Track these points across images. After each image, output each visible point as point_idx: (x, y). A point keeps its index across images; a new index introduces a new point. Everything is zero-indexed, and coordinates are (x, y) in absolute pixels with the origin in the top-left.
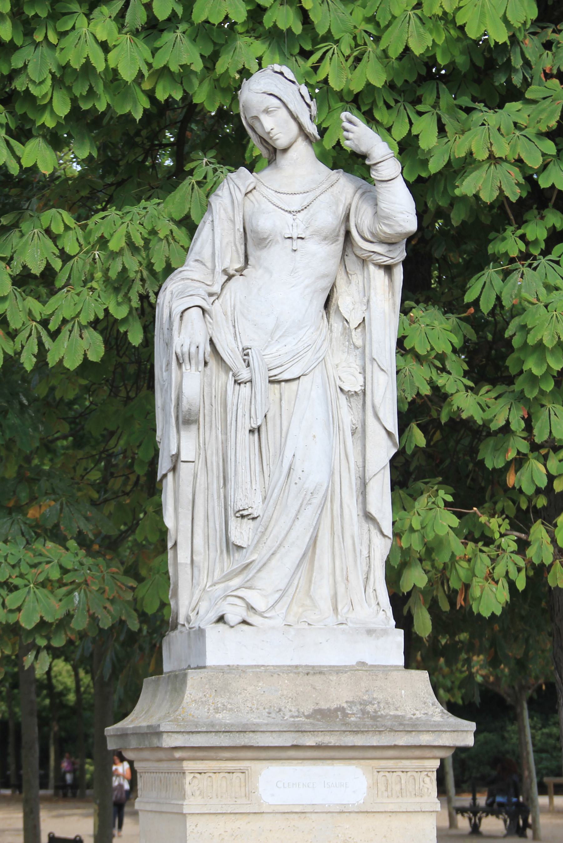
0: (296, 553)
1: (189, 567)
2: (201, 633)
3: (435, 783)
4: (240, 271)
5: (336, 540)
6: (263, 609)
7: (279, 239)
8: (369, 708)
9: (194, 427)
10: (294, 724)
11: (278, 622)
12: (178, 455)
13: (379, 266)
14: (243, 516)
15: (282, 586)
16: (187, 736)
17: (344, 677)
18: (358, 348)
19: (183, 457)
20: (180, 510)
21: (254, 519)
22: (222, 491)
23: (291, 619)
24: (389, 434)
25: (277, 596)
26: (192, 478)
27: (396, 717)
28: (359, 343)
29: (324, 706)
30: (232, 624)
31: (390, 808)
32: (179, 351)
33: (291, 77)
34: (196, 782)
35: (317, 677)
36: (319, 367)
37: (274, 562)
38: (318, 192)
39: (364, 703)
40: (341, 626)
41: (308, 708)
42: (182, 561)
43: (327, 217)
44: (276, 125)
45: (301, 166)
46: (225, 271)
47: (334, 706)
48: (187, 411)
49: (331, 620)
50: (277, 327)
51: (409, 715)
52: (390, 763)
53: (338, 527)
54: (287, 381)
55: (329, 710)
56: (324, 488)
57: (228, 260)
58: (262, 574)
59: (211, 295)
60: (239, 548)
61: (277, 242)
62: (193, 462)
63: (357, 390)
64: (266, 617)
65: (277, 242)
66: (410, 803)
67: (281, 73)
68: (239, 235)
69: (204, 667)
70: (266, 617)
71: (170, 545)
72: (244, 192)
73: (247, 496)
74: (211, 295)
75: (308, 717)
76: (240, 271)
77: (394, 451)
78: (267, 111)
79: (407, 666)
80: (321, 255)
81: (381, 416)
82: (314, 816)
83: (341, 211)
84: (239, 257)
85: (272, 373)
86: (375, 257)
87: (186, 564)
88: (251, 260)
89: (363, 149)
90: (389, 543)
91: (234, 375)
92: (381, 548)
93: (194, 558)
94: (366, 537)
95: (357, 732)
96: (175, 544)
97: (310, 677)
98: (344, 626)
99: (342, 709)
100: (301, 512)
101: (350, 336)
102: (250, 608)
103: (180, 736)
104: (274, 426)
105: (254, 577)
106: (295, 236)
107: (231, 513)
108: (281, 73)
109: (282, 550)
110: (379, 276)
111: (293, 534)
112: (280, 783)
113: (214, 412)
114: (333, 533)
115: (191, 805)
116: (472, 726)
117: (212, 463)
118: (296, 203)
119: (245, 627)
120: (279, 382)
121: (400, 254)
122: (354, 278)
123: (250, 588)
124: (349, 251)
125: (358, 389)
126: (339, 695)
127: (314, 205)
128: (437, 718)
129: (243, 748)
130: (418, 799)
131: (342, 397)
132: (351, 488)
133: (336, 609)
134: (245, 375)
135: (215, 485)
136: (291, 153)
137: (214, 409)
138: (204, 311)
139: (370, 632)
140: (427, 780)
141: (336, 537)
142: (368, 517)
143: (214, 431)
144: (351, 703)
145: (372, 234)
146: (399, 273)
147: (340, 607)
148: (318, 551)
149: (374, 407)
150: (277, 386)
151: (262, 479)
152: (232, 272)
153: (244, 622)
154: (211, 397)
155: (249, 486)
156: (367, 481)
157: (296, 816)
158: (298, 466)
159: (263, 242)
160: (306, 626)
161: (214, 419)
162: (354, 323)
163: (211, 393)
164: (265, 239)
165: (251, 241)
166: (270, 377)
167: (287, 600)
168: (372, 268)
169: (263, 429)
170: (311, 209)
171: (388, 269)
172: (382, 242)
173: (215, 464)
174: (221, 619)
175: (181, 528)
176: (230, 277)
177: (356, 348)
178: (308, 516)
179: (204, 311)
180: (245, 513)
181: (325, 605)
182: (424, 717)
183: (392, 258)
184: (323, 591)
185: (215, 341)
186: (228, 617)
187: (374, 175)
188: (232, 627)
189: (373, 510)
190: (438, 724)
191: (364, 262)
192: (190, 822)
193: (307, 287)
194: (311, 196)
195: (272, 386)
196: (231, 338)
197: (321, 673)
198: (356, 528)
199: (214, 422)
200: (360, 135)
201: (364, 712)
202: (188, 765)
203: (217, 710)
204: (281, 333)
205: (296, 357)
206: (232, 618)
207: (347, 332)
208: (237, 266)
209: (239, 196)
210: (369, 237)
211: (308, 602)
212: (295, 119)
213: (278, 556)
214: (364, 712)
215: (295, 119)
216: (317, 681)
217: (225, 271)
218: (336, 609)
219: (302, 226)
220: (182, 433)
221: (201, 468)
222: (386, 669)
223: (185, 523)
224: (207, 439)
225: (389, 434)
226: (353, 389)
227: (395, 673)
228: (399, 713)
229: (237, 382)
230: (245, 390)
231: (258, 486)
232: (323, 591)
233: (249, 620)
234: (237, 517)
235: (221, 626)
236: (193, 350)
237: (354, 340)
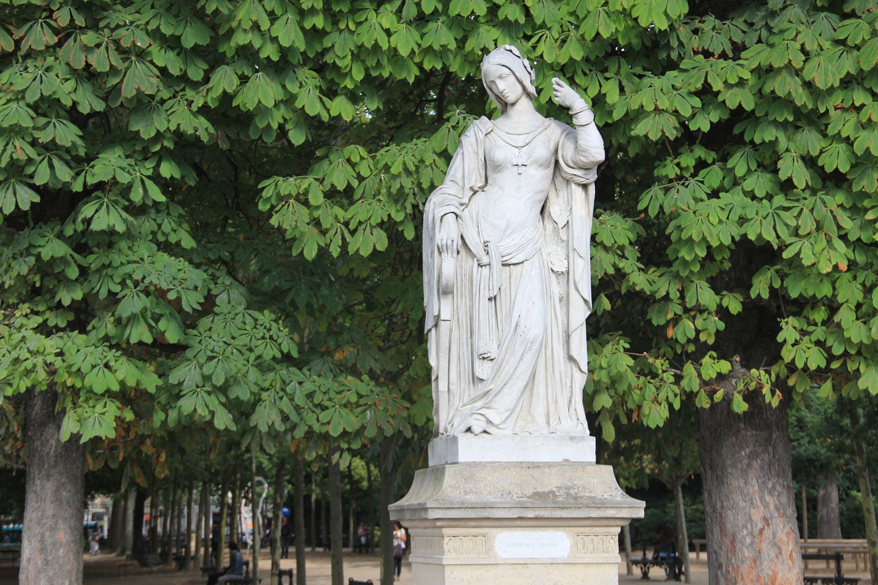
0: (521, 384)
2: (455, 439)
3: (617, 543)
4: (482, 188)
7: (509, 166)
8: (572, 492)
9: (450, 297)
10: (519, 502)
11: (508, 432)
12: (438, 316)
13: (579, 185)
14: (484, 358)
15: (511, 407)
16: (445, 511)
17: (554, 470)
19: (442, 318)
20: (440, 354)
21: (491, 360)
23: (517, 430)
24: (586, 301)
25: (508, 413)
27: (590, 497)
28: (564, 238)
29: (540, 490)
31: (586, 561)
32: (439, 244)
33: (518, 53)
34: (451, 542)
35: (536, 469)
36: (537, 256)
37: (505, 390)
38: (536, 133)
39: (568, 488)
41: (529, 491)
43: (542, 151)
44: (508, 88)
45: (524, 114)
46: (471, 188)
47: (547, 490)
49: (545, 431)
50: (507, 227)
51: (600, 497)
52: (586, 530)
53: (550, 366)
54: (514, 264)
55: (544, 493)
56: (541, 338)
57: (474, 180)
58: (497, 398)
59: (462, 205)
60: (482, 380)
61: (508, 168)
65: (508, 168)
66: (600, 557)
67: (511, 51)
68: (482, 163)
69: (457, 463)
71: (433, 378)
72: (484, 133)
73: (487, 343)
74: (462, 205)
75: (529, 498)
76: (482, 188)
77: (589, 313)
78: (500, 77)
79: (598, 462)
80: (539, 177)
81: (580, 288)
82: (533, 566)
83: (552, 146)
85: (504, 259)
86: (576, 179)
89: (567, 103)
90: (585, 377)
91: (478, 261)
92: (580, 381)
94: (569, 373)
95: (563, 508)
96: (437, 377)
97: (531, 470)
99: (553, 492)
101: (558, 233)
102: (489, 422)
103: (440, 511)
106: (520, 164)
107: (475, 356)
108: (511, 51)
109: (511, 382)
110: (578, 191)
111: (519, 371)
112: (509, 543)
114: (546, 370)
115: (447, 559)
116: (643, 504)
118: (520, 141)
119: (486, 435)
120: (509, 265)
121: (593, 176)
122: (561, 193)
123: (488, 408)
124: (557, 174)
125: (564, 270)
126: (551, 482)
127: (533, 142)
128: (619, 499)
129: (484, 519)
130: (605, 555)
131: (553, 276)
132: (559, 339)
133: (548, 423)
134: (485, 260)
136: (518, 107)
138: (457, 216)
139: (572, 439)
140: (612, 541)
142: (571, 359)
144: (559, 488)
145: (574, 162)
146: (592, 190)
148: (536, 383)
149: (575, 282)
150: (507, 268)
152: (476, 189)
153: (485, 432)
157: (521, 566)
158: (522, 324)
159: (498, 168)
160: (528, 434)
162: (561, 224)
164: (499, 166)
165: (490, 167)
167: (514, 416)
168: (573, 186)
169: (498, 298)
170: (531, 145)
171: (585, 187)
172: (580, 168)
174: (469, 430)
176: (475, 192)
177: (563, 241)
178: (529, 357)
179: (457, 216)
180: (485, 356)
181: (541, 420)
182: (610, 498)
184: (539, 410)
185: (465, 236)
186: (474, 428)
187: (575, 121)
189: (574, 354)
190: (620, 503)
191: (568, 182)
192: (447, 570)
193: (528, 199)
194: (531, 136)
195: (504, 268)
196: (476, 235)
197: (538, 467)
198: (562, 367)
200: (564, 93)
201: (568, 494)
202: (445, 531)
203: (466, 493)
205: (520, 248)
206: (477, 429)
207: (556, 230)
208: (480, 185)
209: (481, 136)
210: (571, 164)
211: (529, 418)
212: (520, 82)
213: (508, 386)
214: (568, 494)
215: (520, 82)
216: (536, 472)
217: (471, 188)
218: (548, 423)
219: (525, 157)
220: (442, 301)
222: (584, 464)
223: (444, 363)
225: (586, 301)
226: (560, 270)
227: (589, 467)
228: (592, 495)
230: (486, 270)
232: (539, 410)
233: (488, 430)
235: (469, 434)
236: (449, 243)
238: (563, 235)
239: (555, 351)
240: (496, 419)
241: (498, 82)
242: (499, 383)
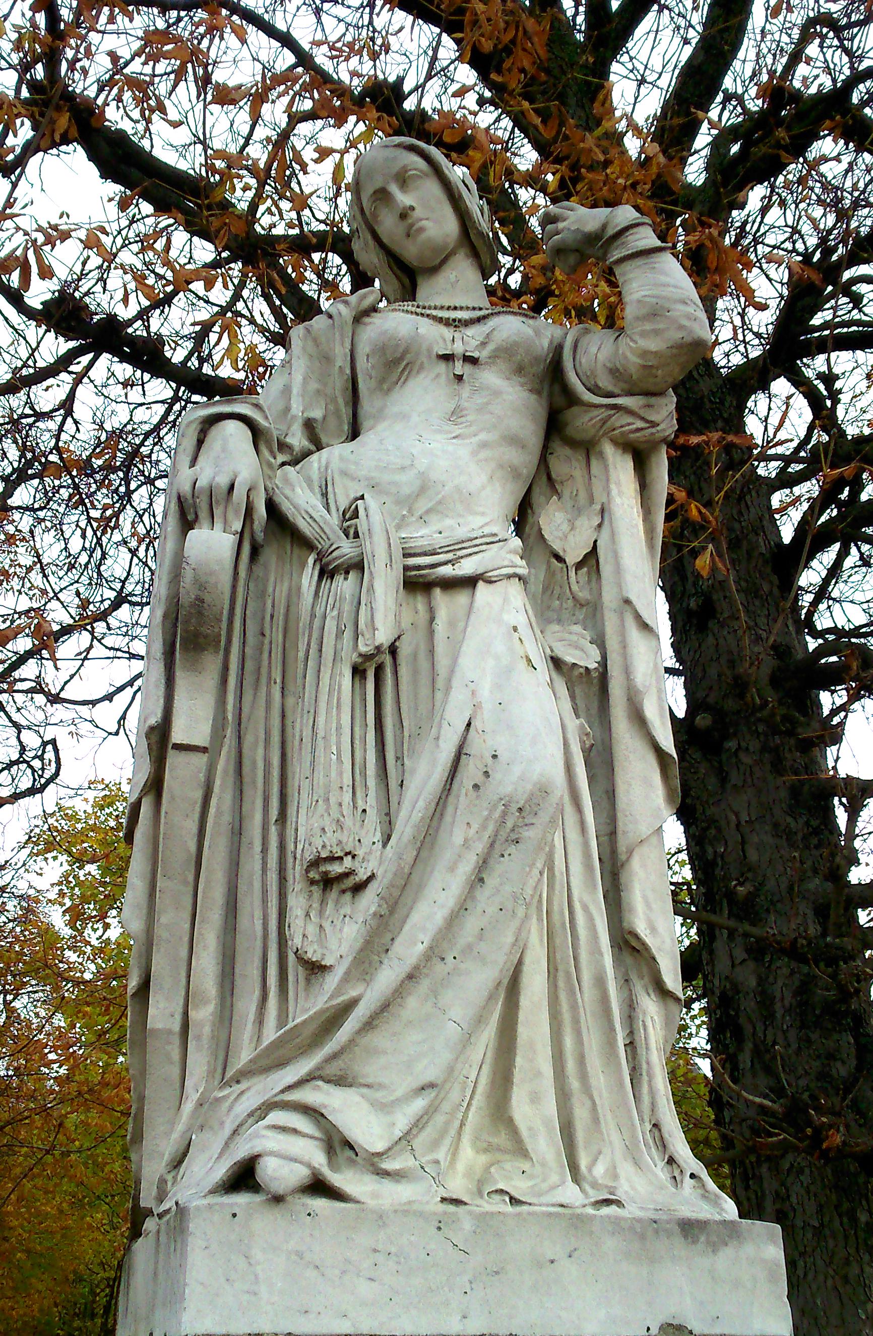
1: (176, 1041)
5: (561, 984)
6: (379, 1147)
9: (212, 663)
14: (328, 882)
18: (582, 605)
19: (178, 736)
22: (273, 830)
23: (457, 1186)
26: (198, 795)
30: (279, 1187)
37: (412, 1003)
40: (606, 1211)
42: (160, 1026)
48: (192, 605)
58: (378, 1039)
62: (204, 750)
63: (589, 666)
64: (386, 1174)
70: (386, 1174)
84: (341, 424)
85: (412, 561)
87: (170, 1032)
88: (365, 424)
93: (191, 1013)
98: (612, 1210)
100: (491, 861)
102: (338, 1144)
104: (415, 672)
105: (352, 1042)
107: (296, 872)
113: (266, 647)
117: (254, 763)
119: (320, 1204)
123: (341, 1081)
125: (592, 666)
132: (589, 867)
135: (258, 817)
137: (267, 641)
141: (561, 975)
142: (629, 946)
143: (263, 690)
145: (614, 372)
147: (583, 1163)
151: (383, 794)
153: (318, 1187)
154: (263, 618)
155: (347, 797)
156: (623, 857)
158: (477, 746)
161: (265, 663)
163: (264, 611)
166: (406, 568)
173: (260, 764)
175: (160, 932)
180: (336, 869)
183: (654, 424)
188: (278, 1199)
193: (484, 445)
199: (264, 671)
204: (430, 505)
206: (278, 1172)
210: (605, 383)
211: (502, 1139)
213: (424, 985)
221: (225, 771)
224: (246, 710)
229: (326, 573)
230: (344, 586)
231: (372, 799)
233: (336, 1179)
234: (312, 882)
237: (575, 587)
238: (577, 583)
239: (577, 906)
240: (366, 1127)
241: (394, 189)
242: (387, 977)
